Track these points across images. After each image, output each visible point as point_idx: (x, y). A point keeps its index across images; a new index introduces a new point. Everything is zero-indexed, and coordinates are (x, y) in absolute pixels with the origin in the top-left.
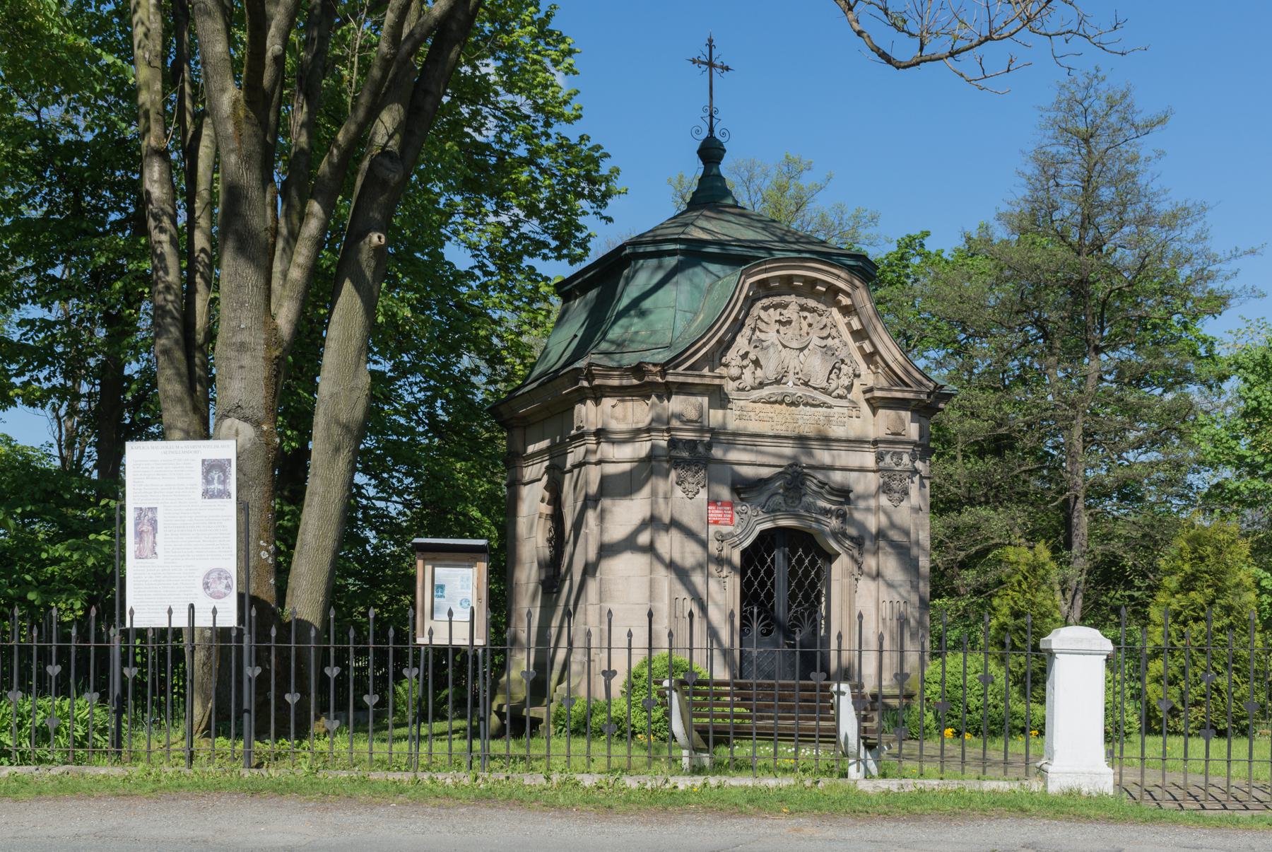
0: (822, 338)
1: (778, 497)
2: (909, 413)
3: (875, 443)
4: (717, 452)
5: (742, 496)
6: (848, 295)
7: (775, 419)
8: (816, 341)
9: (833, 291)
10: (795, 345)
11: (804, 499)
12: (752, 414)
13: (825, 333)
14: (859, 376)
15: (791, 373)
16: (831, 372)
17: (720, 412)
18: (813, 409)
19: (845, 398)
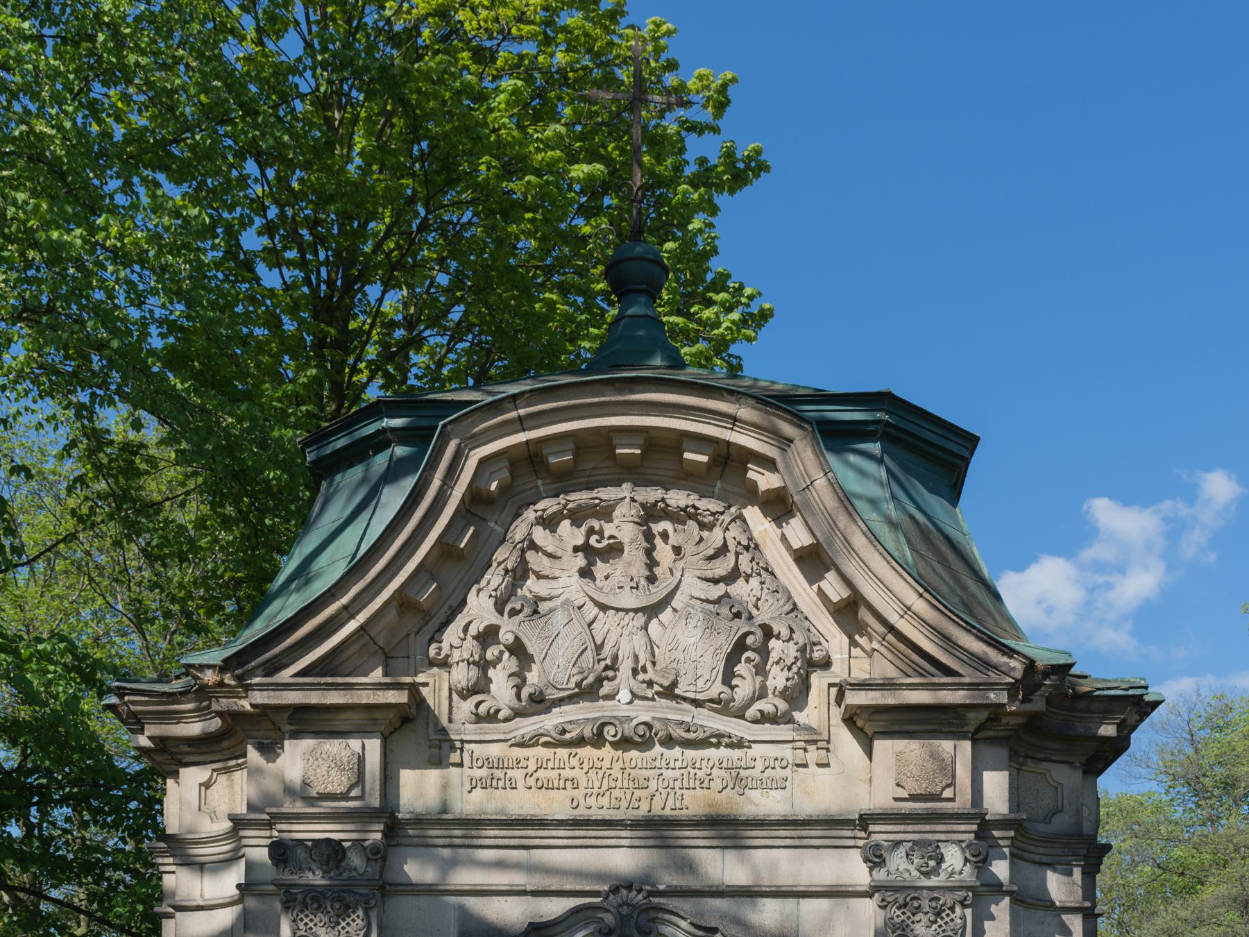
0: (715, 581)
2: (967, 745)
3: (865, 821)
4: (415, 870)
6: (769, 464)
7: (583, 783)
8: (692, 587)
10: (629, 600)
12: (517, 774)
13: (722, 567)
14: (826, 664)
16: (733, 659)
17: (433, 776)
18: (690, 753)
19: (791, 720)
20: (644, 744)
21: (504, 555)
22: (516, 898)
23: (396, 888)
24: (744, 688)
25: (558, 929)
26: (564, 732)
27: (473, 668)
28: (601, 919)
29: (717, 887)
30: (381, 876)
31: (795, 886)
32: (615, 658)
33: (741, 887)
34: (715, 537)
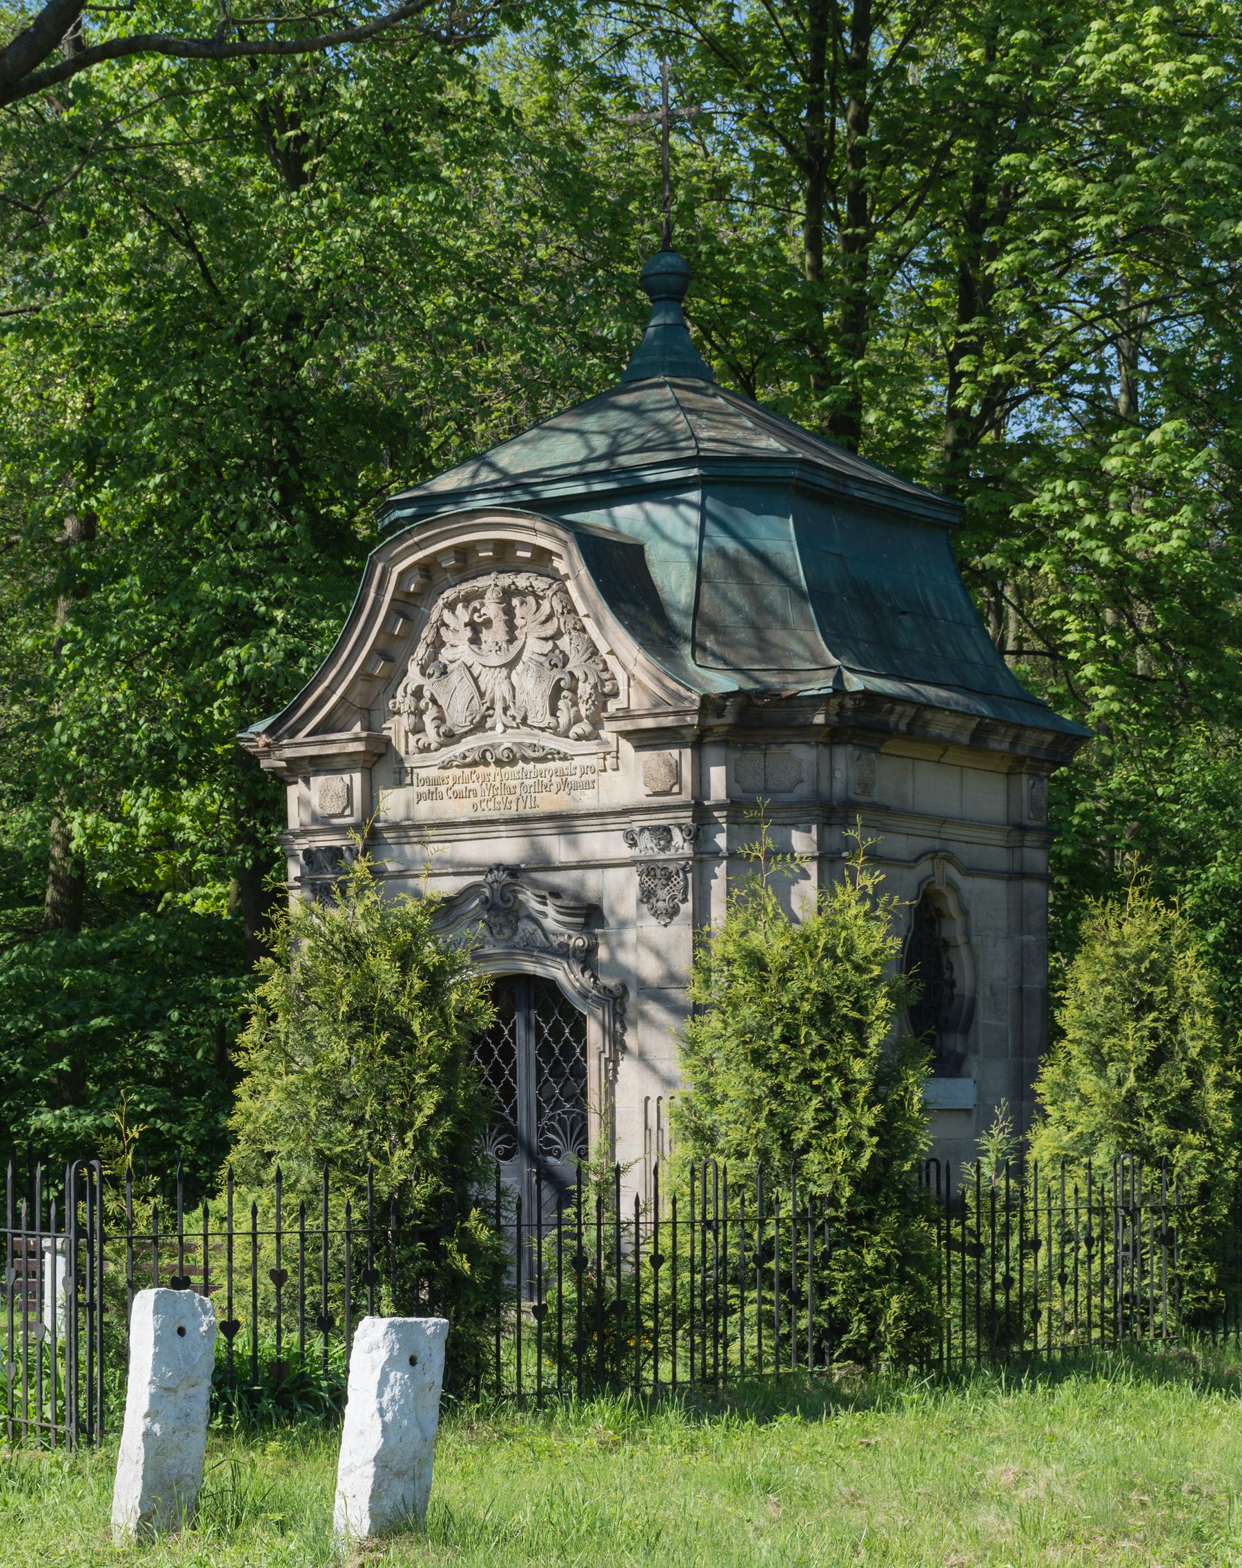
9: (542, 557)
10: (496, 660)
13: (550, 629)
15: (499, 707)
18: (540, 766)
20: (512, 762)
21: (427, 634)
24: (564, 717)
26: (465, 757)
27: (412, 718)
32: (493, 701)
34: (546, 608)
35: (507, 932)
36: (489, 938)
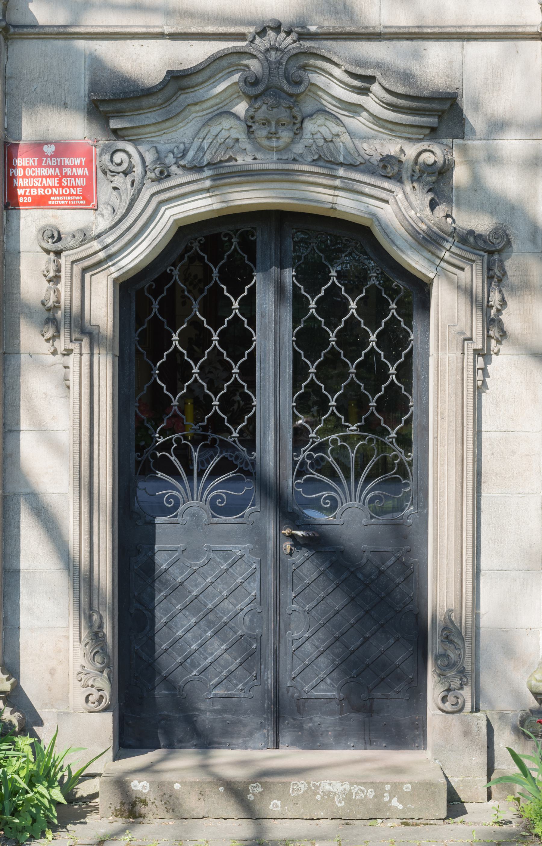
1: (226, 123)
5: (114, 124)
11: (309, 126)
22: (152, 42)
23: (20, 31)
25: (200, 78)
28: (247, 66)
29: (374, 27)
30: (4, 16)
31: (460, 27)
33: (400, 27)
35: (285, 135)
36: (245, 143)
